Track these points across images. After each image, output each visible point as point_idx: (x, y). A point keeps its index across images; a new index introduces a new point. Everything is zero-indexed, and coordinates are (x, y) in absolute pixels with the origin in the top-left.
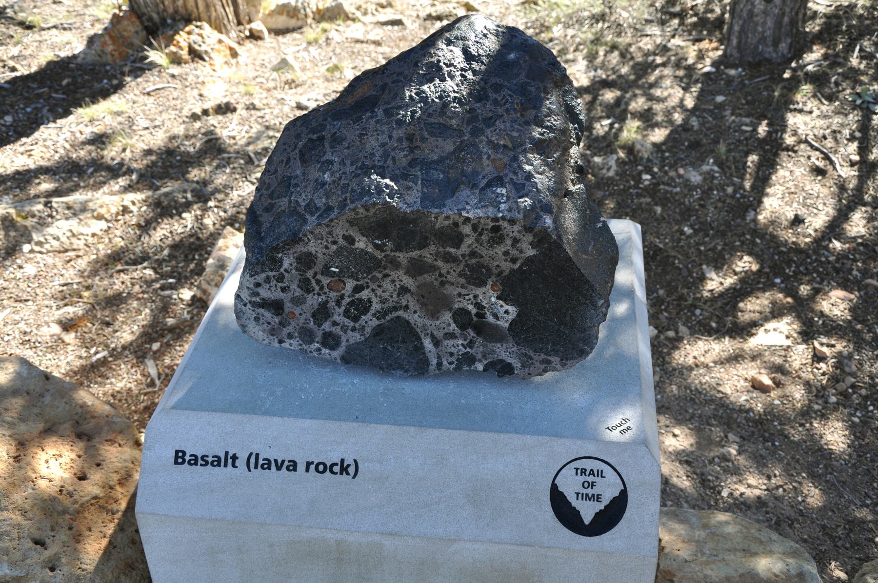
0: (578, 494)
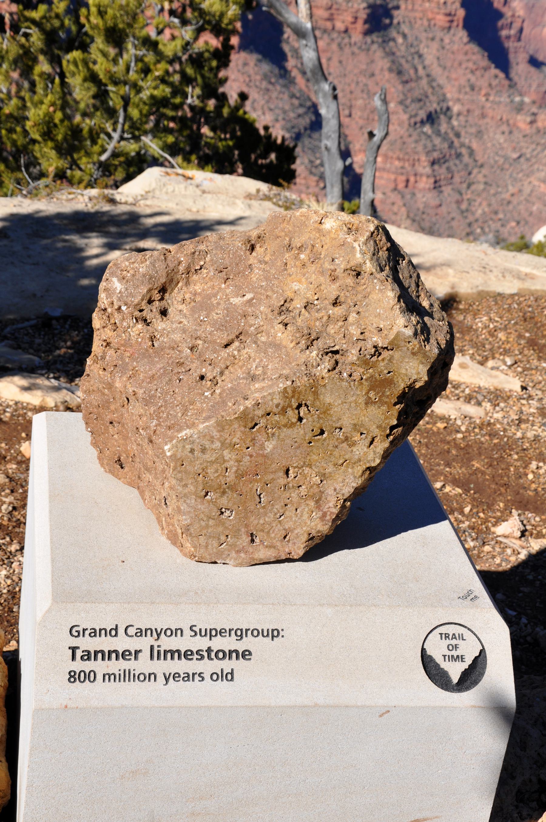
0: (444, 656)
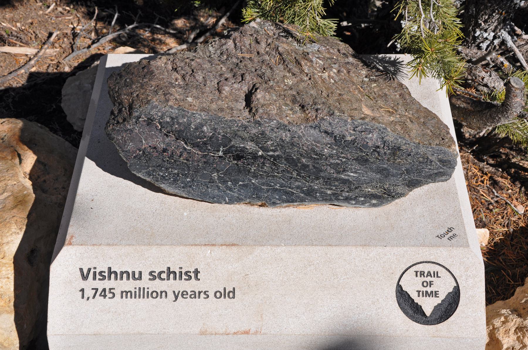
0: (419, 292)
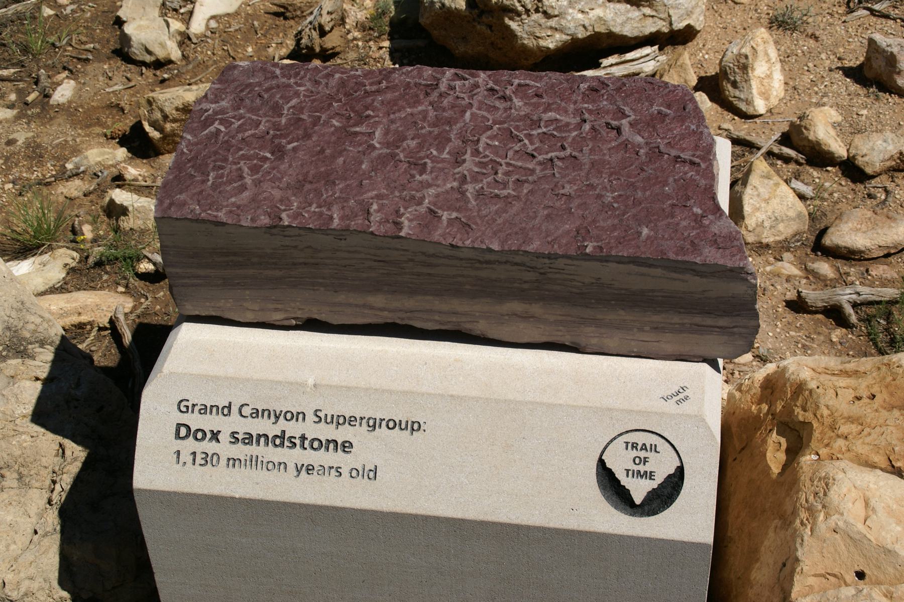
0: (628, 471)
